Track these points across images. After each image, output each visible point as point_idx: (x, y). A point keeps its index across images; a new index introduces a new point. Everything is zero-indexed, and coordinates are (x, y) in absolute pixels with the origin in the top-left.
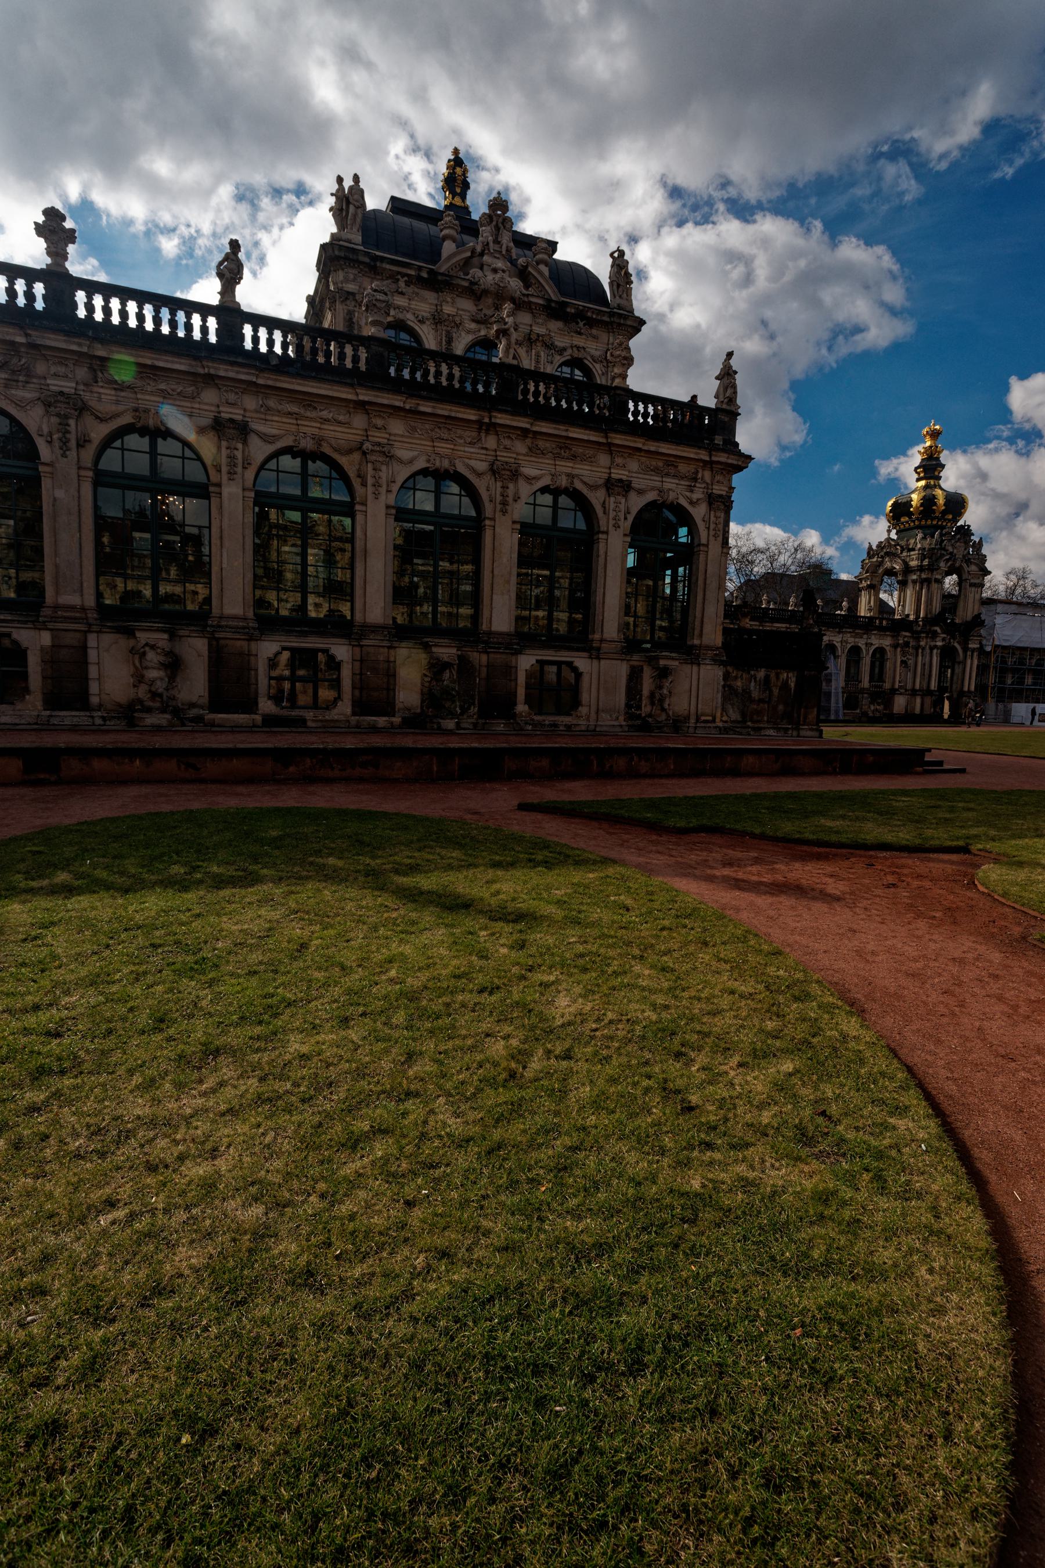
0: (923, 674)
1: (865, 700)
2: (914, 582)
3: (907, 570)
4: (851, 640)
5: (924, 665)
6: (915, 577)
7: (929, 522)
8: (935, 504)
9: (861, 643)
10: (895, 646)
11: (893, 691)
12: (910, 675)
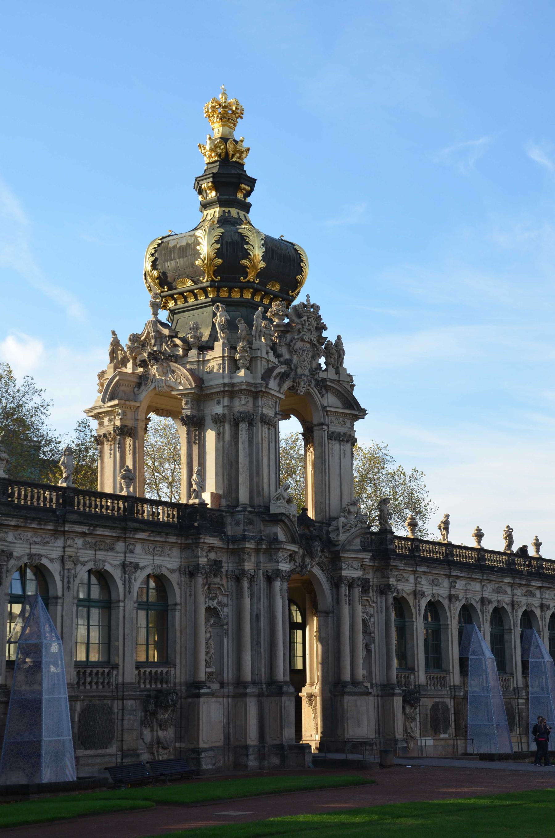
0: (256, 643)
1: (129, 714)
3: (202, 392)
4: (86, 555)
5: (256, 618)
6: (219, 410)
7: (236, 295)
8: (246, 255)
9: (112, 564)
10: (191, 572)
11: (195, 688)
12: (228, 646)
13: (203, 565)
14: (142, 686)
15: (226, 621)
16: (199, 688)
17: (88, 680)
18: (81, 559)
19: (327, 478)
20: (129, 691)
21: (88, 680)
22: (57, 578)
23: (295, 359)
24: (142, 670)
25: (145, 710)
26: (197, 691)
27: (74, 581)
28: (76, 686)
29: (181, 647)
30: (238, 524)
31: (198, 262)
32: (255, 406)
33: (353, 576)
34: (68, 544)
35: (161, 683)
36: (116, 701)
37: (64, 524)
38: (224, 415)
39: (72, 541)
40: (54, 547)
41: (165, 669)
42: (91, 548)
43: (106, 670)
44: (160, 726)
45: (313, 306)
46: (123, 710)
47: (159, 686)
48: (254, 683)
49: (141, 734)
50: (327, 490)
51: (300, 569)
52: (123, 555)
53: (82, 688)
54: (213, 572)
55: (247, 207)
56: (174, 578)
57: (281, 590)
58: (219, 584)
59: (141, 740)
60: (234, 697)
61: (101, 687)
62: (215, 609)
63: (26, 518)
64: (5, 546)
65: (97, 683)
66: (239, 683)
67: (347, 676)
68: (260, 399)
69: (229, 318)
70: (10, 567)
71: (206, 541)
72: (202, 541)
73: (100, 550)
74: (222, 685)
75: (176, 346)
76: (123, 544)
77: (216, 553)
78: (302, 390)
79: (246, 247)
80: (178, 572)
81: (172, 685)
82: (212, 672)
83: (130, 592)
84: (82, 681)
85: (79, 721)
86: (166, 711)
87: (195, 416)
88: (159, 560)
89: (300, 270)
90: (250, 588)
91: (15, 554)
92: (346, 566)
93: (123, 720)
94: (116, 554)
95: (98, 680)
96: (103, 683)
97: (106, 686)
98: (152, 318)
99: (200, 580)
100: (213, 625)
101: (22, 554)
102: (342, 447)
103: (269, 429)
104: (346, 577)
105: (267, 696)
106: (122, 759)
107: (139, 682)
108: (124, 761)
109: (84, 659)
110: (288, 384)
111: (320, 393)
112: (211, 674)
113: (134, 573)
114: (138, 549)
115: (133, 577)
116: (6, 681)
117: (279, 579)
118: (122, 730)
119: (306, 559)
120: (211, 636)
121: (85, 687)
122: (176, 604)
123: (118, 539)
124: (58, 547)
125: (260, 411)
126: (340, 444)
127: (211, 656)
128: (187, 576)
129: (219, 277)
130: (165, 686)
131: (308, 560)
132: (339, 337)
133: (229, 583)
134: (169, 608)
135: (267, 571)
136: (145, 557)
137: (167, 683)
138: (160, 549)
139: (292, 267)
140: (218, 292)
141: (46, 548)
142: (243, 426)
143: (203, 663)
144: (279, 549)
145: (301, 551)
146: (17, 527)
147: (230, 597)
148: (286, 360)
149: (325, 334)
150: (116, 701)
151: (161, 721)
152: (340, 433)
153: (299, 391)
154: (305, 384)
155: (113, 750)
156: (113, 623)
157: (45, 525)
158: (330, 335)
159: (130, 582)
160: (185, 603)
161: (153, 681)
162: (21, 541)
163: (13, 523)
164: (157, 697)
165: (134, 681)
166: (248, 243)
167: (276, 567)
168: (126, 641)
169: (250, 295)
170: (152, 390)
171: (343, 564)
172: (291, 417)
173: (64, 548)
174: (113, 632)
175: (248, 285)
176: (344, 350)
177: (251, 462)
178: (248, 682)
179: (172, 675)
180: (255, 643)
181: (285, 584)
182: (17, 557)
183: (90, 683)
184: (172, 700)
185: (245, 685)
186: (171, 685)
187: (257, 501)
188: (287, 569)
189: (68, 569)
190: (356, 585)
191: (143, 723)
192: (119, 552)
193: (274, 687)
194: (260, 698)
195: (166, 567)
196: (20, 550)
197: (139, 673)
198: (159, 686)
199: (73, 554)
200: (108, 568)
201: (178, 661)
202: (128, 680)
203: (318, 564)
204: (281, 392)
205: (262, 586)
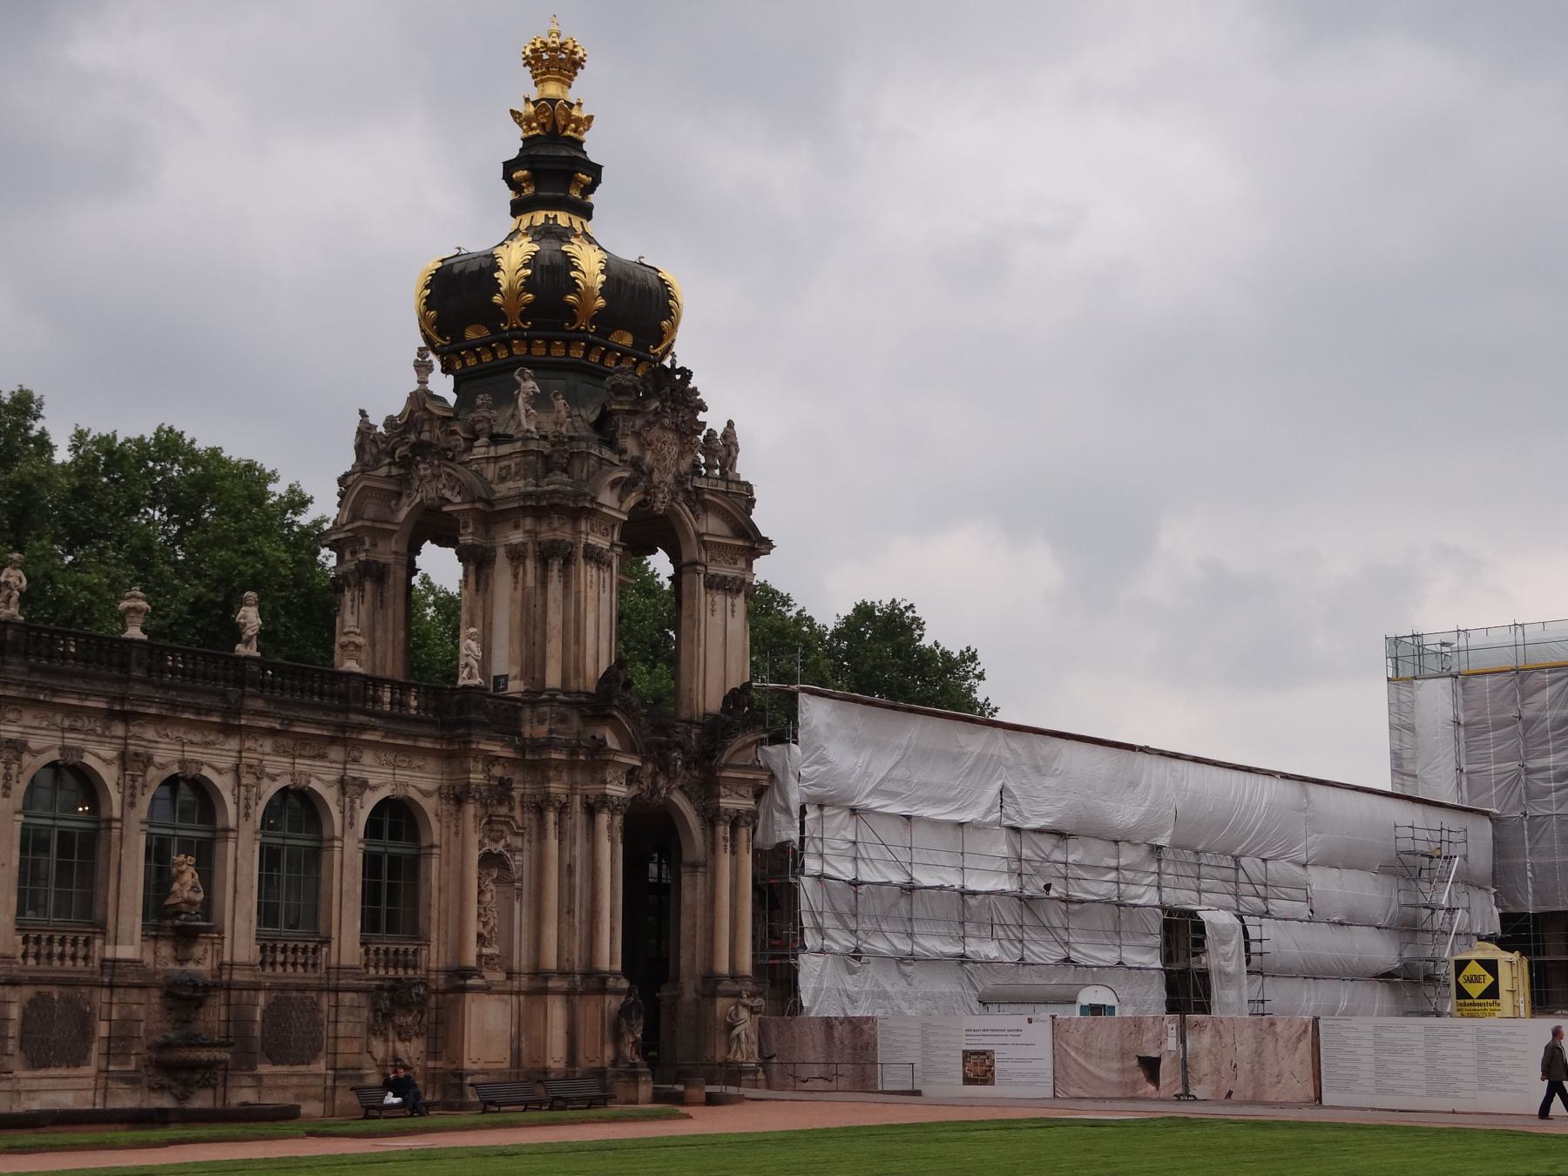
0: (566, 910)
5: (567, 871)
6: (517, 537)
7: (558, 351)
8: (573, 286)
9: (322, 778)
10: (457, 797)
11: (459, 979)
12: (521, 913)
14: (372, 971)
16: (465, 978)
17: (280, 958)
21: (280, 958)
25: (375, 1009)
30: (541, 722)
31: (497, 299)
35: (405, 967)
37: (238, 715)
42: (285, 753)
43: (311, 945)
44: (399, 1034)
45: (683, 371)
46: (337, 1007)
48: (562, 973)
53: (269, 970)
55: (586, 212)
56: (430, 805)
57: (610, 827)
60: (527, 993)
61: (300, 969)
62: (500, 855)
63: (173, 705)
66: (538, 973)
67: (723, 967)
70: (148, 778)
71: (481, 747)
73: (301, 756)
74: (510, 975)
75: (454, 433)
79: (573, 274)
83: (352, 824)
84: (269, 960)
85: (263, 1020)
88: (403, 775)
90: (560, 823)
91: (157, 759)
96: (304, 965)
99: (471, 809)
100: (497, 881)
105: (582, 994)
107: (366, 966)
112: (491, 957)
113: (360, 795)
122: (432, 846)
123: (332, 741)
130: (411, 972)
131: (662, 782)
132: (730, 424)
137: (415, 967)
140: (529, 347)
143: (473, 938)
144: (607, 762)
146: (158, 719)
149: (701, 417)
155: (320, 1066)
158: (712, 421)
159: (352, 809)
160: (448, 843)
163: (152, 711)
164: (392, 989)
166: (576, 268)
173: (240, 752)
175: (580, 335)
177: (565, 624)
183: (283, 964)
186: (421, 973)
187: (573, 685)
191: (373, 1030)
198: (401, 972)
199: (256, 762)
200: (315, 785)
201: (434, 936)
202: (345, 961)
203: (681, 788)
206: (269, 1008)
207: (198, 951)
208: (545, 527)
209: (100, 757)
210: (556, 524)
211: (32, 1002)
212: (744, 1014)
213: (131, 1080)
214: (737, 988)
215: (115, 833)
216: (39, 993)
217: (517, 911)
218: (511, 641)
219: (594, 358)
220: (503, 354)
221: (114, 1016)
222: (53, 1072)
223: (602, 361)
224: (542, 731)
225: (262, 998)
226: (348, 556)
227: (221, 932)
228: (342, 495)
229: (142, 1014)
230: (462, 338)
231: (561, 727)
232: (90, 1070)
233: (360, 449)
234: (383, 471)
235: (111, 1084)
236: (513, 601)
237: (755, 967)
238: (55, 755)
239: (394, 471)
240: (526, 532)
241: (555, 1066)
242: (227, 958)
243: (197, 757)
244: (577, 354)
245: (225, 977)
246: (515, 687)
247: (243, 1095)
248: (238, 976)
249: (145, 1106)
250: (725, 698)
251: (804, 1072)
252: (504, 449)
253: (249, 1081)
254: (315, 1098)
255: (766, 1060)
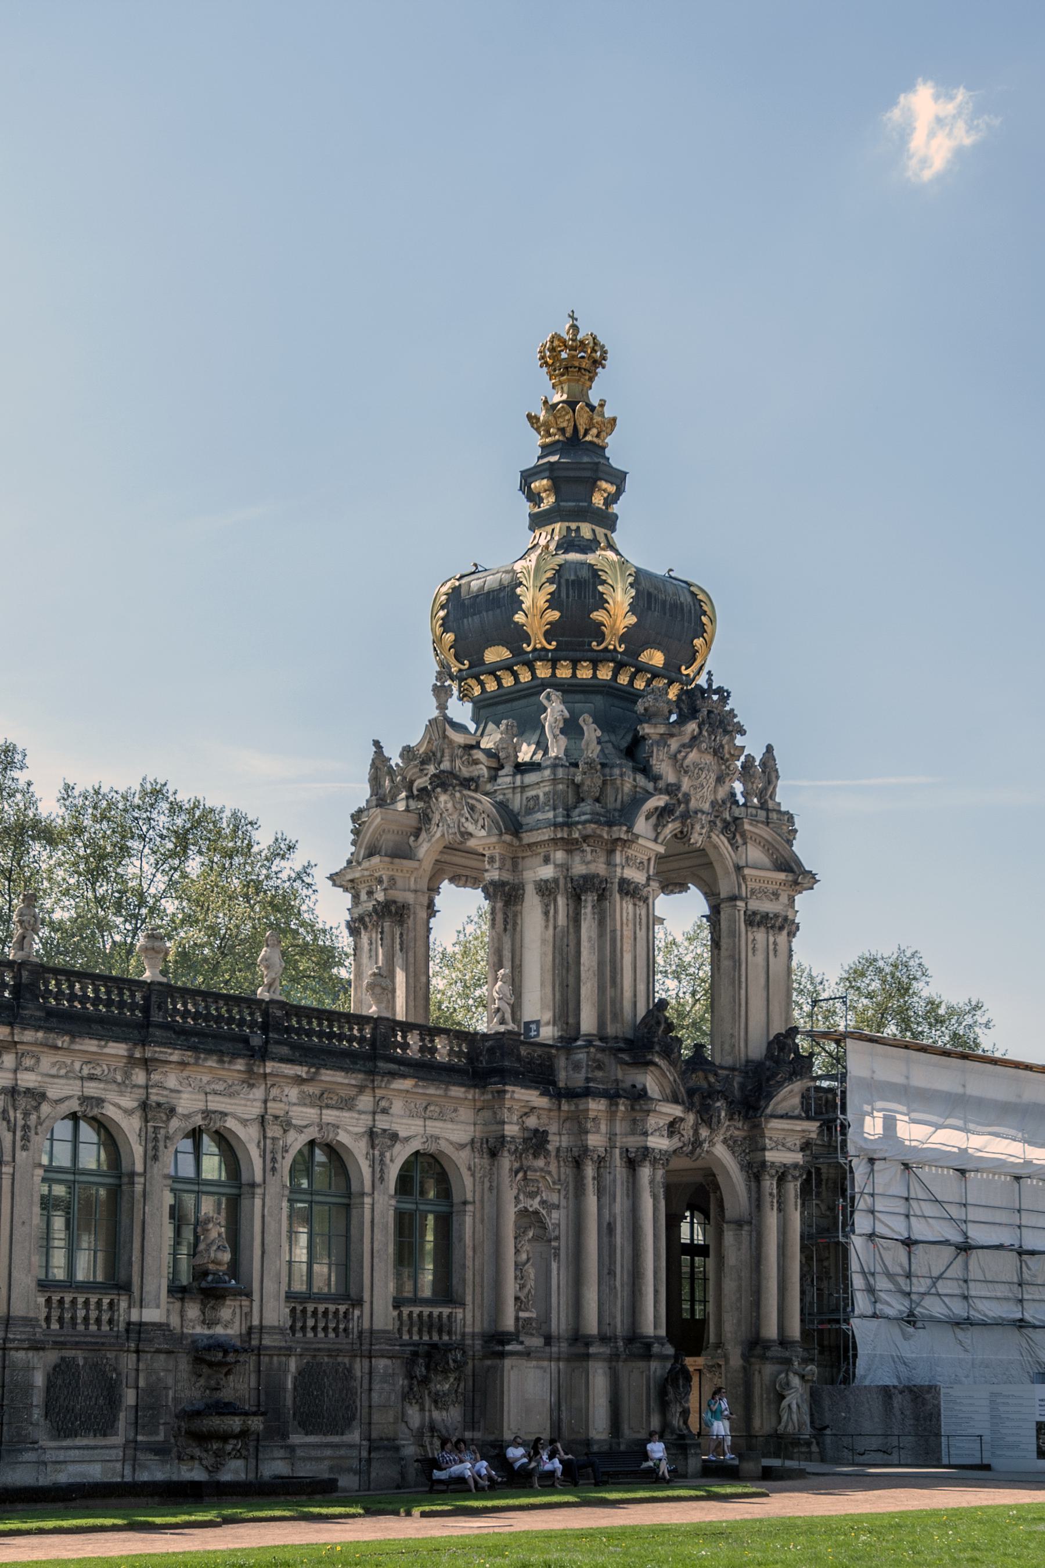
0: (607, 1271)
1: (382, 1381)
2: (546, 889)
4: (304, 1114)
5: (608, 1230)
6: (547, 872)
7: (585, 673)
9: (350, 1130)
10: (492, 1148)
11: (496, 1342)
12: (559, 1274)
13: (512, 1137)
14: (406, 1337)
15: (557, 1233)
16: (503, 1343)
17: (310, 1323)
18: (294, 1122)
19: (743, 992)
20: (380, 1344)
21: (310, 1323)
22: (255, 1153)
23: (686, 784)
24: (406, 1311)
25: (410, 1376)
26: (501, 1348)
27: (283, 1158)
28: (288, 1331)
29: (474, 1275)
30: (577, 1067)
32: (610, 863)
33: (785, 1161)
34: (271, 1097)
35: (440, 1332)
36: (358, 1359)
38: (556, 881)
39: (279, 1091)
40: (248, 1100)
41: (446, 1311)
43: (342, 1308)
44: (436, 1402)
46: (370, 1373)
47: (436, 1338)
48: (604, 1339)
49: (403, 1414)
50: (743, 1013)
51: (690, 1147)
52: (370, 1117)
53: (299, 1335)
54: (531, 1151)
56: (462, 1159)
57: (652, 1182)
58: (542, 1170)
59: (403, 1424)
61: (332, 1335)
62: (536, 1213)
64: (163, 1096)
65: (325, 1329)
66: (578, 1338)
67: (771, 1331)
68: (618, 853)
69: (567, 714)
70: (171, 1131)
72: (508, 1096)
73: (328, 1107)
74: (548, 1340)
75: (476, 762)
76: (372, 1099)
77: (539, 1118)
78: (697, 838)
80: (469, 1147)
81: (459, 1337)
82: (529, 1319)
83: (382, 1179)
84: (299, 1324)
85: (295, 1388)
86: (447, 1378)
87: (508, 883)
88: (435, 1127)
89: (700, 630)
90: (598, 1178)
92: (774, 1145)
93: (370, 1390)
94: (356, 1116)
95: (327, 1323)
96: (335, 1329)
97: (342, 1334)
98: (435, 713)
99: (506, 1162)
101: (192, 1110)
102: (771, 939)
103: (635, 905)
104: (773, 1163)
105: (625, 1360)
106: (370, 1453)
107: (400, 1330)
108: (373, 1455)
109: (304, 1288)
110: (671, 828)
111: (731, 845)
112: (528, 1320)
114: (398, 1106)
115: (388, 1155)
116: (168, 1317)
117: (647, 1164)
118: (370, 1407)
119: (701, 1131)
120: (528, 1259)
121: (304, 1335)
122: (465, 1203)
123: (361, 1089)
124: (255, 1100)
125: (618, 874)
126: (768, 933)
127: (529, 1291)
128: (485, 1156)
129: (554, 643)
130: (446, 1338)
131: (704, 1133)
133: (562, 1170)
134: (455, 1209)
135: (627, 1150)
136: (410, 1122)
138: (437, 1109)
139: (686, 624)
140: (554, 668)
141: (233, 1101)
142: (589, 899)
143: (511, 1302)
145: (691, 1118)
146: (183, 1064)
147: (563, 1193)
148: (668, 785)
149: (739, 740)
150: (358, 1359)
151: (437, 1394)
152: (767, 914)
153: (692, 841)
154: (703, 828)
155: (354, 1436)
156: (354, 1231)
157: (230, 1062)
158: (751, 744)
159: (382, 1162)
160: (482, 1201)
161: (425, 1329)
162: (190, 1089)
164: (429, 1355)
165: (391, 1328)
167: (642, 1144)
168: (376, 1260)
169: (610, 674)
170: (438, 839)
171: (767, 1141)
172: (689, 888)
173: (265, 1102)
174: (353, 1246)
175: (607, 655)
176: (776, 771)
177: (601, 964)
178: (590, 1336)
179: (458, 1321)
180: (606, 1271)
181: (660, 1173)
182: (184, 1115)
183: (314, 1329)
184: (455, 1361)
185: (587, 1341)
187: (610, 1030)
188: (664, 1147)
189: (273, 1139)
190: (790, 1178)
191: (407, 1396)
192: (364, 1112)
193: (638, 1345)
194: (614, 1364)
195: (447, 1140)
196: (189, 1103)
197: (400, 1315)
198: (436, 1338)
199: (281, 1113)
200: (343, 1137)
201: (469, 1299)
202: (378, 1325)
203: (725, 1141)
204: (660, 841)
205: (618, 1176)
206: (301, 1373)
207: (225, 1313)
208: (577, 859)
209: (121, 1109)
210: (589, 857)
211: (56, 1367)
212: (796, 1381)
213: (160, 1451)
214: (787, 1354)
215: (138, 1188)
216: (63, 1359)
217: (554, 1273)
218: (542, 984)
219: (623, 679)
220: (525, 676)
221: (142, 1383)
222: (79, 1441)
223: (631, 682)
224: (578, 1080)
225: (293, 1364)
226: (363, 896)
227: (249, 1295)
228: (356, 832)
229: (170, 1382)
230: (482, 662)
231: (599, 1074)
232: (118, 1440)
233: (375, 781)
234: (401, 806)
235: (140, 1456)
236: (544, 941)
237: (803, 1332)
238: (74, 1106)
239: (413, 804)
240: (556, 866)
241: (597, 1437)
242: (256, 1322)
243: (221, 1107)
244: (605, 673)
245: (255, 1342)
246: (547, 1033)
247: (275, 1467)
248: (267, 1342)
249: (175, 1478)
250: (770, 1044)
251: (862, 1444)
252: (531, 778)
253: (281, 1453)
254: (350, 1470)
255: (819, 1430)
